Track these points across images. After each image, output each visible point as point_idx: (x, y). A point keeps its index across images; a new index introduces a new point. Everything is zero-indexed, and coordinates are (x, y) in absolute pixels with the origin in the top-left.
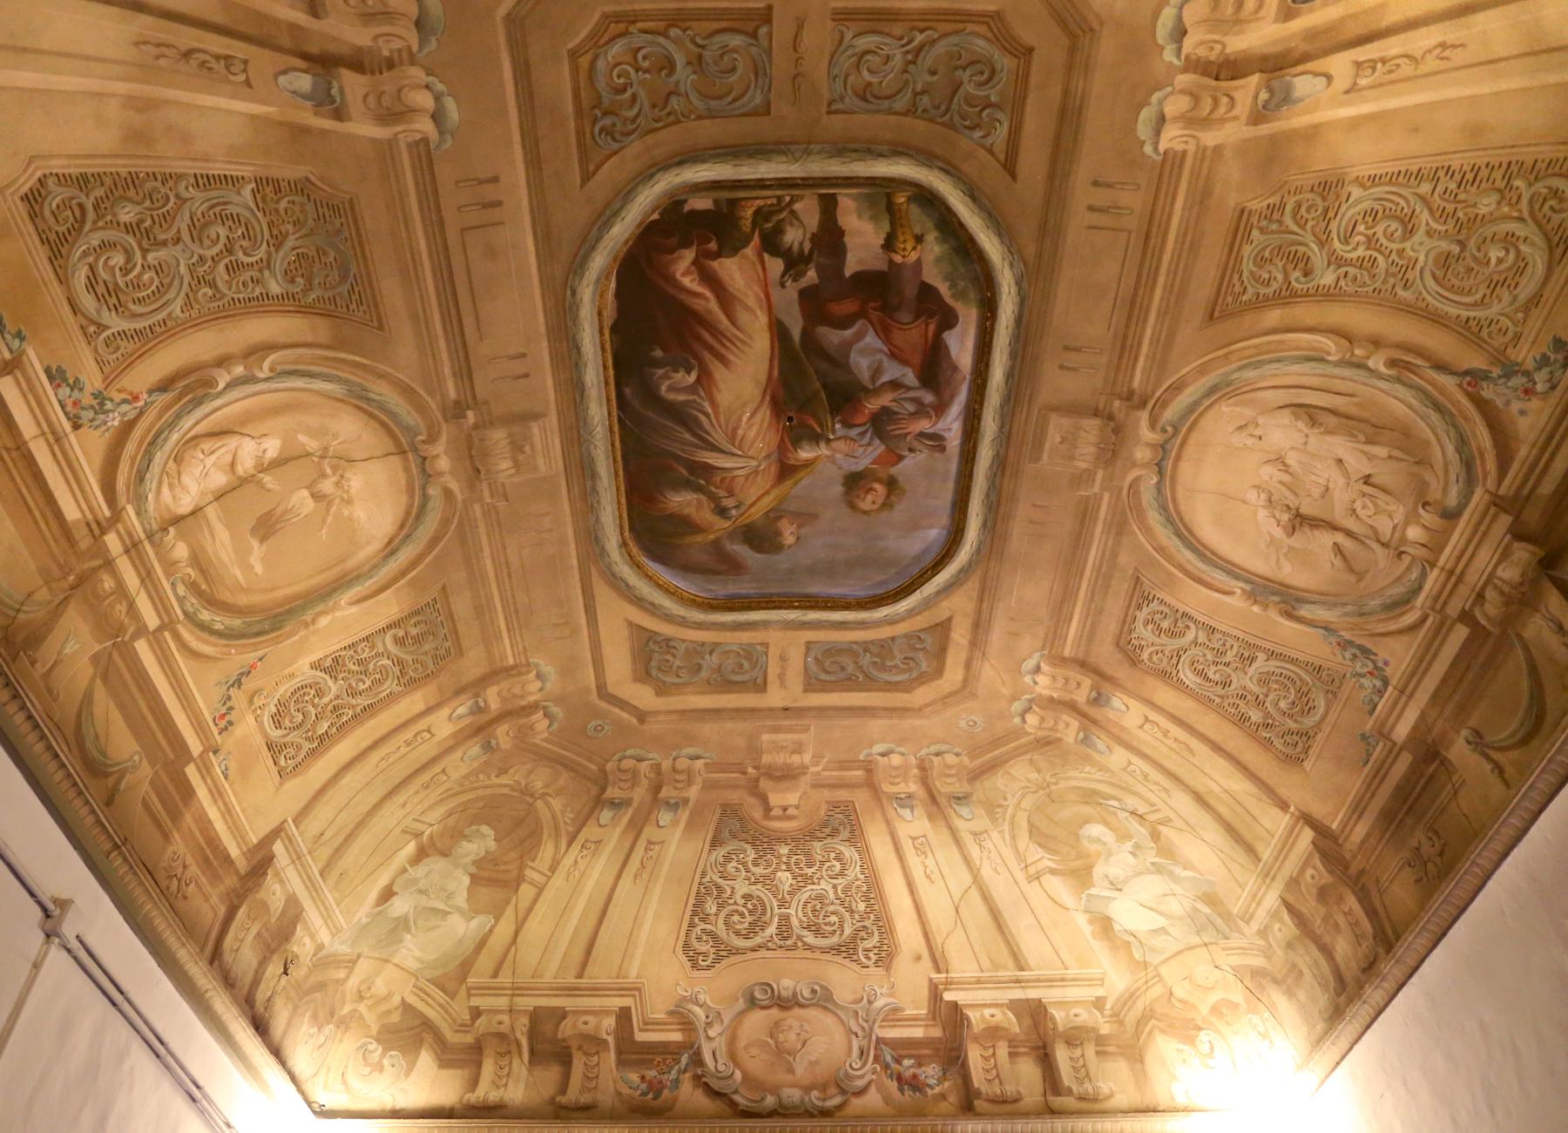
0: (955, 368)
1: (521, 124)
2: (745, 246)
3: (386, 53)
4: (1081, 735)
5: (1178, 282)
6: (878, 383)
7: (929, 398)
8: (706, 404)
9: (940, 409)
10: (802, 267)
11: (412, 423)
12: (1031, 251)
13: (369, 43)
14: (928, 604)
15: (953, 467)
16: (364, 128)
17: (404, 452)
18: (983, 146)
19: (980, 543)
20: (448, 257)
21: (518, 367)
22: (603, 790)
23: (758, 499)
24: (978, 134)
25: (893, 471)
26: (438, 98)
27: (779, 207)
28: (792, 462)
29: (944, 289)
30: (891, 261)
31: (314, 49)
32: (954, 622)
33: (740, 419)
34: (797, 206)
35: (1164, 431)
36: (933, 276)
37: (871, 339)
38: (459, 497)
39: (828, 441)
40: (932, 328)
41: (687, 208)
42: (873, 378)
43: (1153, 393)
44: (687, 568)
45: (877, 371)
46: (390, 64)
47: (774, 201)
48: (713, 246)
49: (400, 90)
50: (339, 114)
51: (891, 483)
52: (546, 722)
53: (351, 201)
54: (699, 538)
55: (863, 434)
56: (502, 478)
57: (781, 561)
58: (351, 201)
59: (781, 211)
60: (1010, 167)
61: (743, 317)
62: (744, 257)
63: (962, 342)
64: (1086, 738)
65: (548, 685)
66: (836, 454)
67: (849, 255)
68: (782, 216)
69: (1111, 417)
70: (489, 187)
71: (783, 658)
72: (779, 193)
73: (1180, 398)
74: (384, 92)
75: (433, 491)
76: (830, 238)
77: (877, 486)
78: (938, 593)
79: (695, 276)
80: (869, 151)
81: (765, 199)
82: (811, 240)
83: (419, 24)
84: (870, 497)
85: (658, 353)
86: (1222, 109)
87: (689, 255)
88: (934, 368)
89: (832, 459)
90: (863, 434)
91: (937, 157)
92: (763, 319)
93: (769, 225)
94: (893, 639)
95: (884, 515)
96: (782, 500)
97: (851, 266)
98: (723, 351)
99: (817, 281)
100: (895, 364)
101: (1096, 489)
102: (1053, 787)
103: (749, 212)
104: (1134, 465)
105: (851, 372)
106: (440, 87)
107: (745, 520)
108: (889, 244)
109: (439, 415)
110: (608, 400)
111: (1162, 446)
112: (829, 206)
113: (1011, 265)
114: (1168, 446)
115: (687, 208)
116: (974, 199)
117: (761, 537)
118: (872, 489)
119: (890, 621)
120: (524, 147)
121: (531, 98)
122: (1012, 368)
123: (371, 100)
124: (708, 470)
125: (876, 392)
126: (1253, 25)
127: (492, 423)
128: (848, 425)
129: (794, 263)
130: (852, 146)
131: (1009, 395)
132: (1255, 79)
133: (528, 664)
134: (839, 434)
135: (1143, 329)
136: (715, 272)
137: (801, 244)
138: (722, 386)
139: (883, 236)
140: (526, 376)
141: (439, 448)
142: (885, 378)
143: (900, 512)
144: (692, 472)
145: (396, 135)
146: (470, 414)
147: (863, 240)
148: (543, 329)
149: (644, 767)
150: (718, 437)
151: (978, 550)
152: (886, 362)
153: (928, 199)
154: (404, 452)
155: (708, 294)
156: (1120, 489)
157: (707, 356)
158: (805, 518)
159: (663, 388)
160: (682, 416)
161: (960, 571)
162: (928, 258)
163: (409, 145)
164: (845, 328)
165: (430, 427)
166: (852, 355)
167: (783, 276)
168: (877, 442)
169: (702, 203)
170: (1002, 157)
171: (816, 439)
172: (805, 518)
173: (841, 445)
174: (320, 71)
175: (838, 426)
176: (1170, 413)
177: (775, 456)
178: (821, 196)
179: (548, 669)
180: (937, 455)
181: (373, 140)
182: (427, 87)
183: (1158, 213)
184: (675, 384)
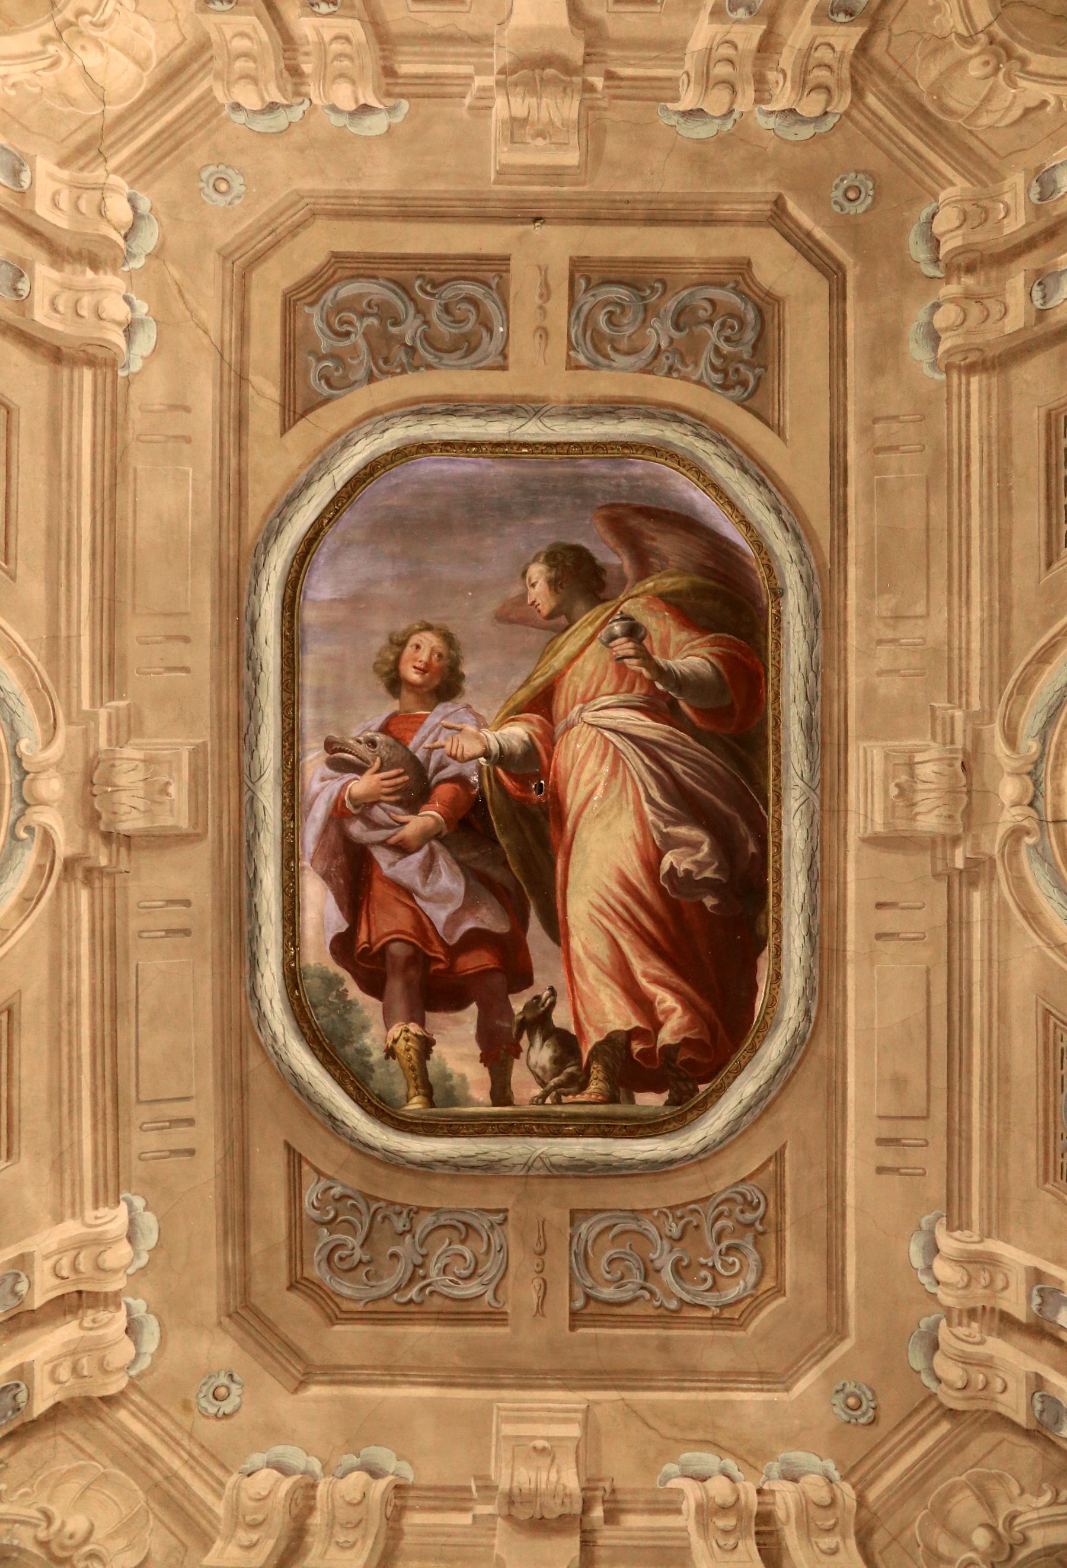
0: (326, 877)
1: (844, 1226)
2: (599, 1044)
3: (975, 1325)
4: (26, 177)
5: (65, 1050)
6: (426, 848)
7: (357, 829)
8: (651, 817)
9: (339, 814)
10: (529, 1016)
11: (1036, 865)
12: (255, 1061)
13: (991, 1340)
14: (321, 462)
15: (308, 714)
16: (1016, 1257)
17: (1056, 822)
18: (329, 1178)
19: (255, 590)
20: (950, 1088)
21: (889, 921)
22: (863, 47)
23: (582, 649)
24: (337, 1191)
25: (393, 706)
26: (929, 1268)
27: (558, 1093)
28: (535, 717)
29: (354, 991)
30: (422, 1024)
31: (1048, 1346)
32: (277, 425)
33: (606, 789)
34: (538, 1091)
35: (29, 829)
36: (369, 1006)
37: (439, 915)
38: (997, 727)
39: (486, 754)
40: (363, 936)
41: (665, 1096)
42: (432, 855)
43: (58, 888)
44: (687, 523)
45: (428, 868)
46: (972, 1314)
47: (564, 1099)
48: (637, 1047)
49: (967, 1286)
50: (1037, 1276)
51: (395, 683)
52: (938, 227)
53: (1046, 1180)
54: (668, 583)
55: (440, 767)
56: (935, 751)
57: (547, 531)
58: (1046, 1180)
59: (557, 1086)
60: (295, 1159)
61: (601, 948)
62: (598, 1030)
63: (322, 916)
64: (16, 174)
65: (921, 314)
66: (473, 733)
67: (473, 1031)
68: (556, 1080)
69: (108, 837)
70: (889, 1163)
71: (544, 333)
72: (559, 1109)
73: (21, 886)
74: (985, 1287)
75: (1031, 746)
76: (497, 1051)
77: (414, 677)
78: (307, 484)
79: (659, 1008)
80: (457, 1167)
81: (574, 1104)
82: (520, 1050)
83: (935, 1346)
84: (424, 656)
85: (709, 902)
86: (65, 1262)
87: (666, 1037)
88: (355, 876)
89: (481, 723)
90: (440, 767)
91: (377, 1161)
92: (576, 944)
93: (569, 1070)
94: (371, 378)
95: (403, 625)
96: (548, 649)
97: (470, 1015)
98: (627, 899)
99: (511, 997)
100: (405, 880)
101: (103, 713)
102: (49, 29)
103: (593, 1086)
104: (58, 765)
105: (459, 863)
106: (924, 1279)
107: (600, 612)
108: (426, 1045)
109: (1000, 870)
110: (779, 846)
111: (28, 805)
112: (501, 1093)
113: (274, 1038)
114: (18, 806)
115: (665, 1096)
116: (331, 1116)
117: (580, 578)
118: (423, 671)
119: (378, 417)
120: (844, 1201)
121: (828, 1251)
122: (251, 895)
123: (1000, 1283)
124: (652, 707)
125: (427, 837)
126: (56, 1353)
127: (933, 841)
128: (460, 780)
129: (539, 1021)
130: (477, 1173)
131: (250, 852)
132: (38, 1302)
133: (948, 369)
135: (93, 977)
136: (635, 1013)
137: (531, 1045)
138: (630, 845)
139: (434, 1055)
140: (880, 905)
141: (1010, 817)
142: (418, 856)
143: (381, 627)
144: (673, 704)
145: (981, 1241)
146: (960, 864)
147: (457, 1046)
148: (851, 970)
149: (784, 97)
150: (636, 761)
151: (257, 572)
153: (381, 1109)
154: (1056, 822)
155: (643, 982)
156: (69, 722)
157: (647, 892)
158: (514, 614)
159: (705, 848)
160: (684, 803)
161: (279, 532)
162: (378, 1029)
163: (969, 1227)
164: (471, 931)
165: (1015, 853)
166: (462, 890)
167: (553, 1004)
168: (420, 754)
169: (650, 1101)
170: (306, 1168)
171: (503, 758)
172: (514, 614)
173: (472, 747)
174: (1047, 1325)
175: (475, 779)
176: (28, 858)
177: (560, 727)
178: (509, 1102)
179: (918, 353)
180: (337, 736)
181: (1008, 1241)
182: (938, 1283)
183: (110, 1133)
184: (691, 854)
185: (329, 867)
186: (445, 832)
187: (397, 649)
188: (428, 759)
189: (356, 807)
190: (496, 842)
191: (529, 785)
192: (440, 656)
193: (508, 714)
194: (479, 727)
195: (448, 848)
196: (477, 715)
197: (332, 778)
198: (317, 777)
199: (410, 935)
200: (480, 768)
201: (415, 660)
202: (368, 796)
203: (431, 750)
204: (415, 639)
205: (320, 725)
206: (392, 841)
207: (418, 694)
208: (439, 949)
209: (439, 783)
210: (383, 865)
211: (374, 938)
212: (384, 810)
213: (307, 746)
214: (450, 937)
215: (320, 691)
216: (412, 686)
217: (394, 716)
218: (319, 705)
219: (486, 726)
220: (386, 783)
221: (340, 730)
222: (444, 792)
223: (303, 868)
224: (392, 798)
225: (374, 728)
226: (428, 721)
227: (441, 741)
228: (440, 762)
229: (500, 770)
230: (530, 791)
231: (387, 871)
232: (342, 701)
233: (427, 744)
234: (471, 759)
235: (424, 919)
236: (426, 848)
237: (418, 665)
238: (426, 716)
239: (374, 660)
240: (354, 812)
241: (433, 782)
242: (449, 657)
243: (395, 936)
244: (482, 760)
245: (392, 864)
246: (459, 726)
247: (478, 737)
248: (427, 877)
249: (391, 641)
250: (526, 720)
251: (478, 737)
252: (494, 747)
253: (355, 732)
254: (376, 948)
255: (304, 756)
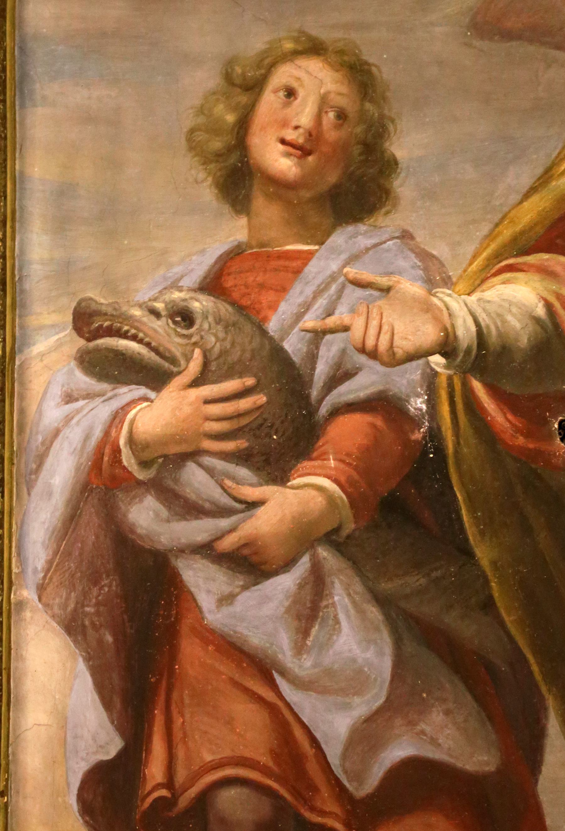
0: (73, 627)
6: (305, 562)
7: (145, 516)
9: (105, 479)
25: (235, 231)
37: (333, 724)
39: (447, 347)
40: (155, 771)
45: (309, 611)
51: (237, 179)
55: (341, 375)
63: (63, 720)
77: (279, 162)
84: (304, 114)
88: (139, 627)
90: (341, 375)
95: (256, 42)
100: (255, 639)
105: (382, 601)
118: (302, 151)
125: (306, 537)
134: (413, 373)
142: (285, 583)
152: (280, 643)
166: (386, 665)
168: (294, 345)
171: (484, 357)
173: (412, 331)
175: (418, 404)
180: (101, 299)
185: (80, 604)
186: (350, 527)
187: (244, 99)
188: (312, 358)
189: (144, 464)
190: (467, 552)
191: (546, 423)
192: (342, 115)
193: (498, 256)
194: (430, 283)
195: (356, 565)
196: (425, 256)
197: (90, 396)
198: (56, 391)
199: (264, 770)
200: (431, 378)
201: (284, 124)
202: (172, 439)
203: (318, 335)
204: (283, 75)
205: (65, 272)
206: (228, 543)
207: (288, 204)
208: (332, 807)
209: (337, 411)
210: (206, 601)
211: (181, 776)
212: (210, 471)
213: (33, 321)
214: (359, 777)
215: (64, 192)
216: (278, 186)
217: (235, 253)
218: (61, 224)
219: (447, 282)
220: (216, 409)
221: (109, 285)
222: (348, 433)
223: (21, 605)
224: (229, 446)
225: (187, 282)
226: (312, 268)
227: (341, 315)
228: (338, 365)
229: (477, 386)
230: (550, 437)
231: (214, 615)
232: (113, 217)
233: (310, 321)
234: (411, 357)
235: (298, 733)
236: (305, 562)
237: (291, 135)
238: (311, 254)
239: (188, 123)
240: (141, 475)
241: (324, 410)
242: (362, 115)
243: (229, 772)
244: (437, 360)
245: (226, 600)
246: (384, 281)
247: (428, 308)
248: (306, 633)
249: (228, 77)
250: (545, 272)
251: (428, 308)
252: (465, 332)
253: (145, 291)
254: (184, 802)
255: (26, 343)
